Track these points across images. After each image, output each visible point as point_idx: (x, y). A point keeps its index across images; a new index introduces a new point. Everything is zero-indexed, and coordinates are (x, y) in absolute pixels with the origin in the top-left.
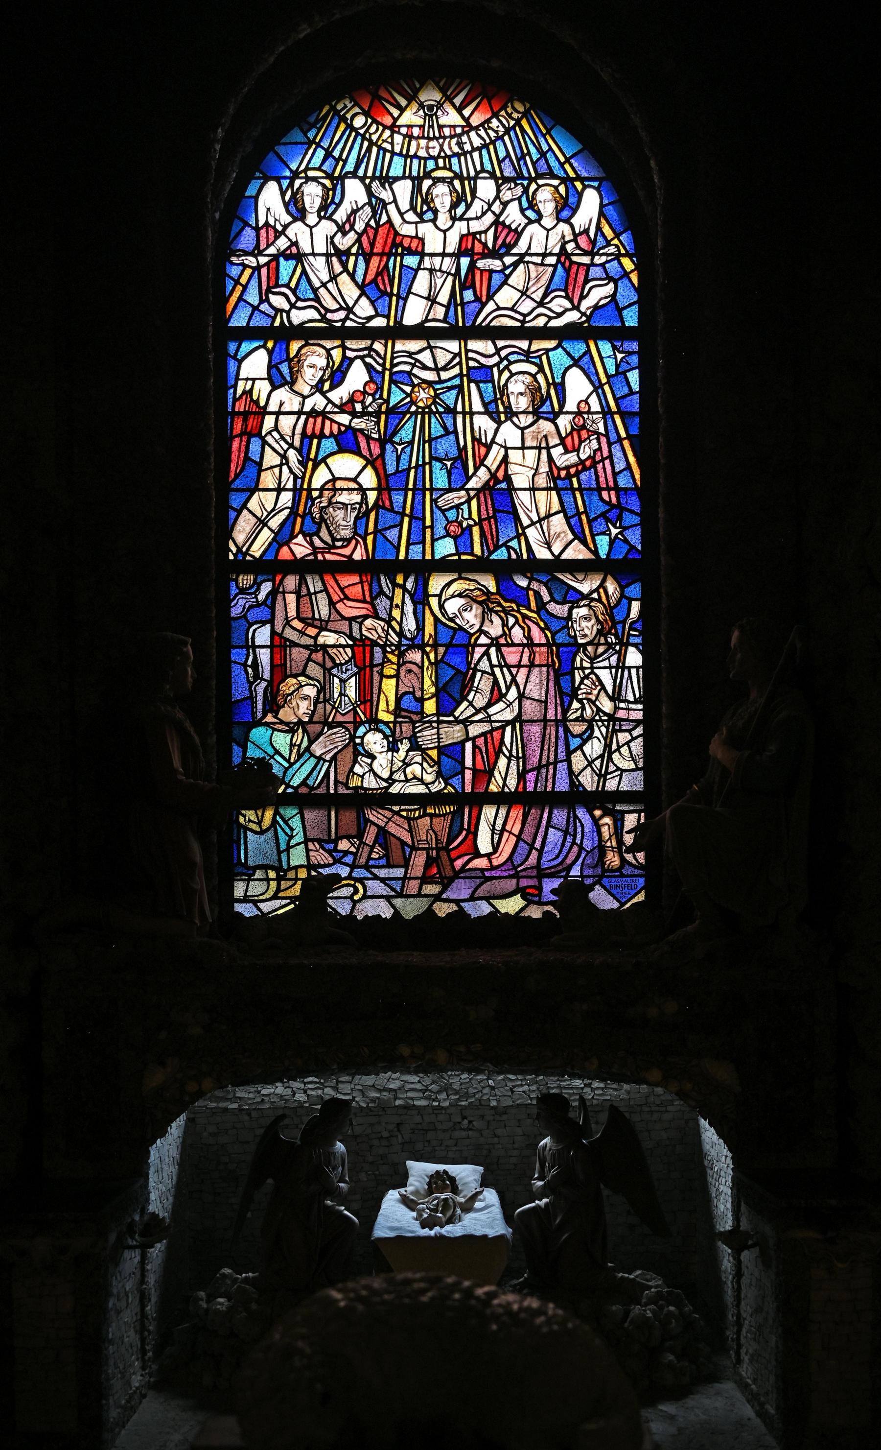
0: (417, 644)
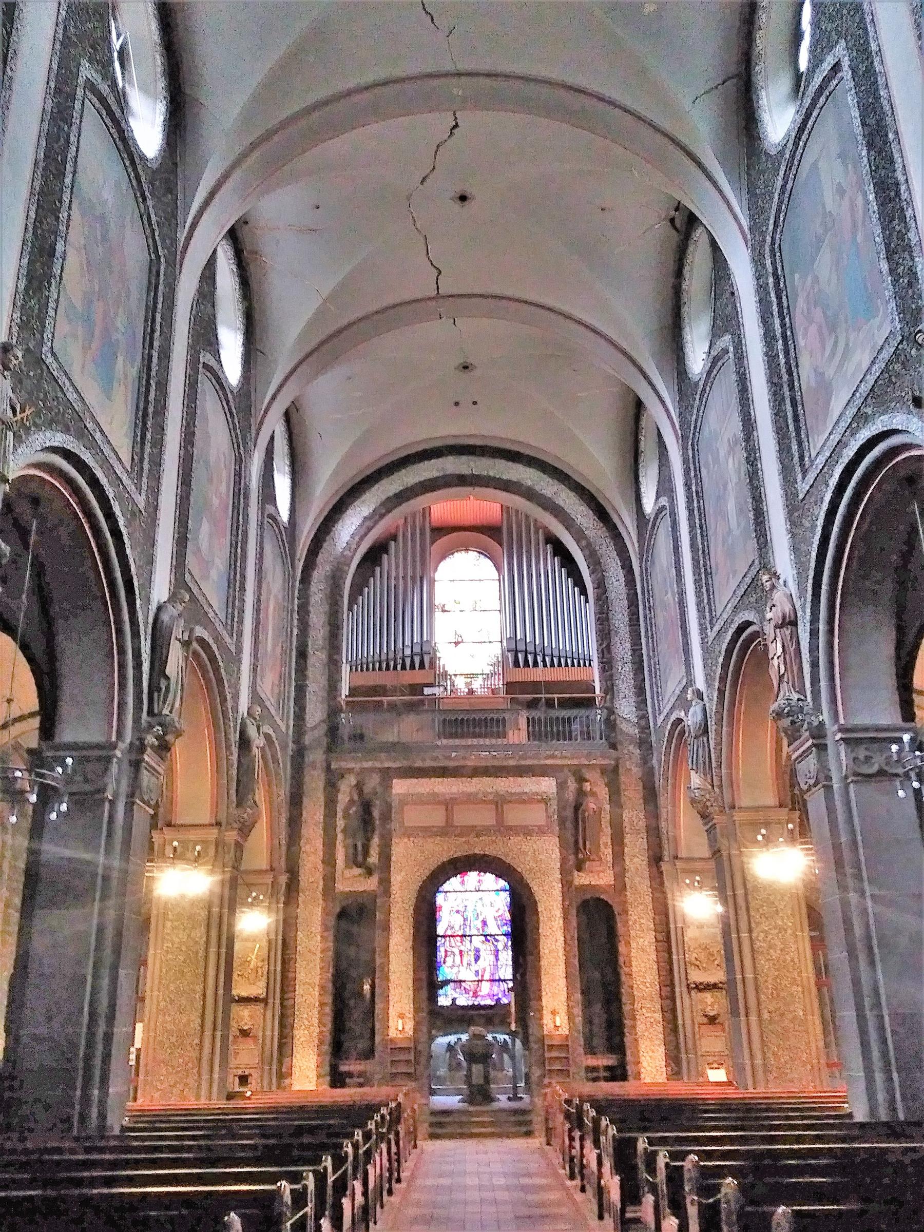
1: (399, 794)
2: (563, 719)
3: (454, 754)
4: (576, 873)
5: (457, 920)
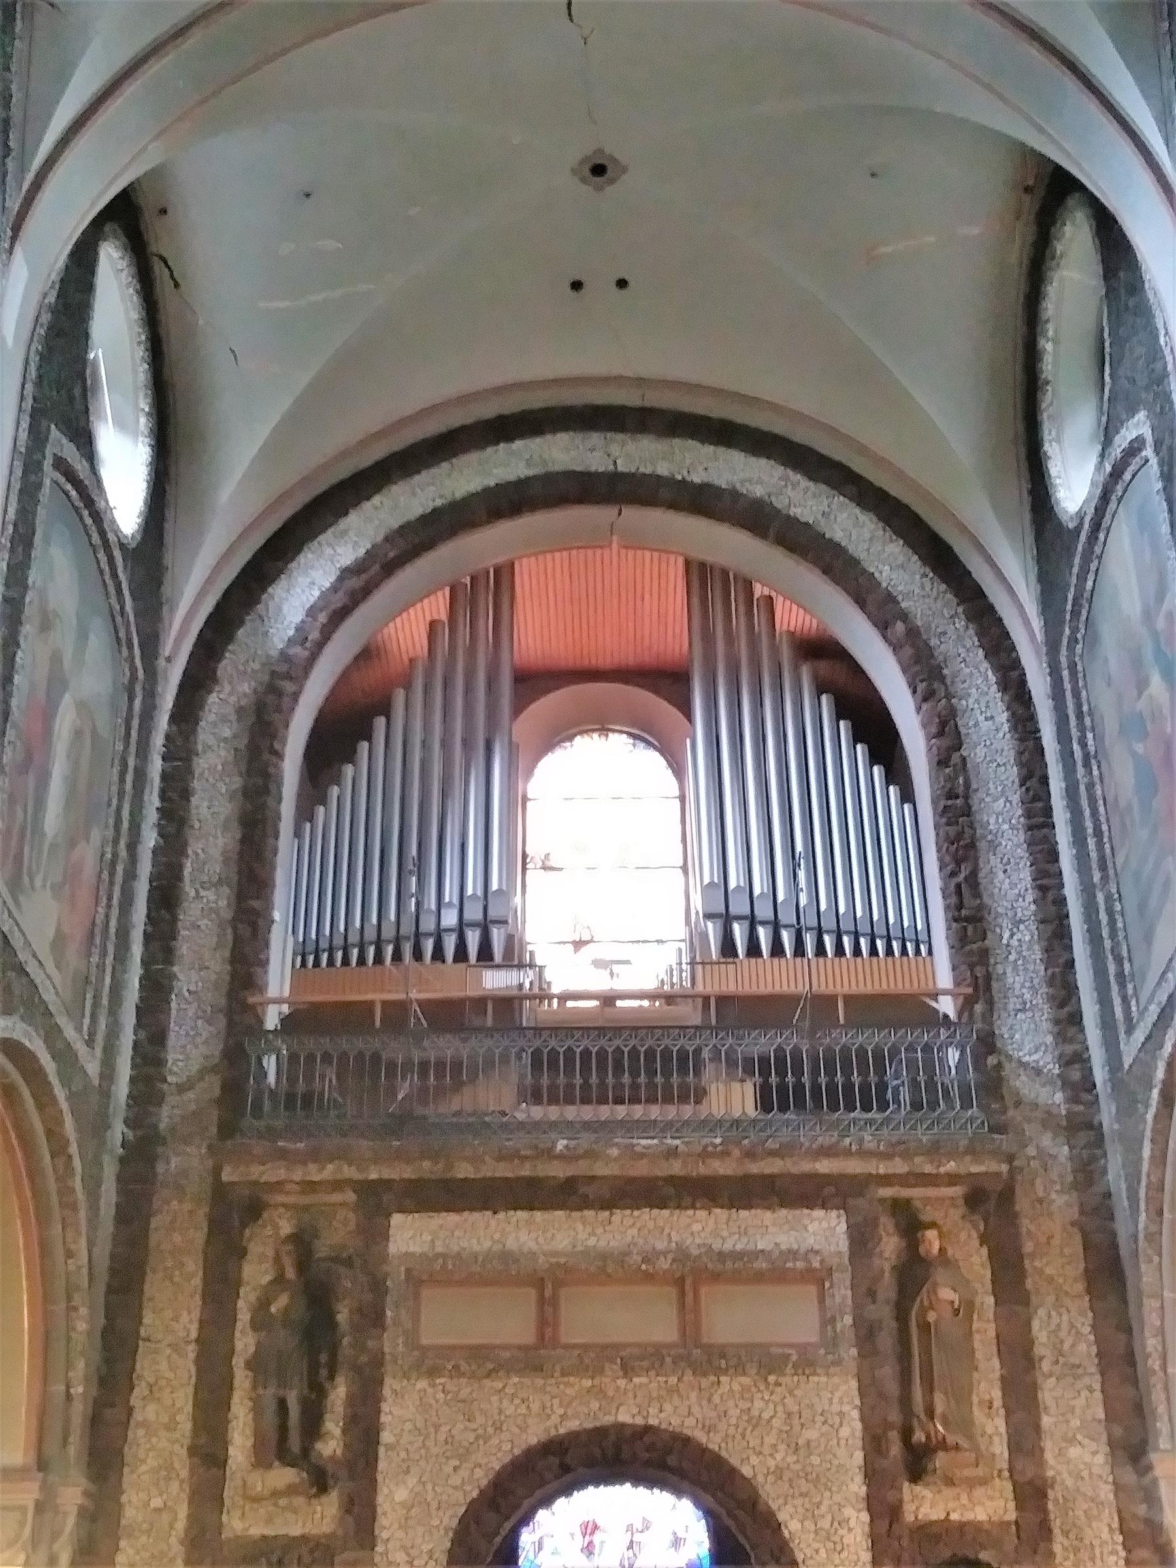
2: (862, 1053)
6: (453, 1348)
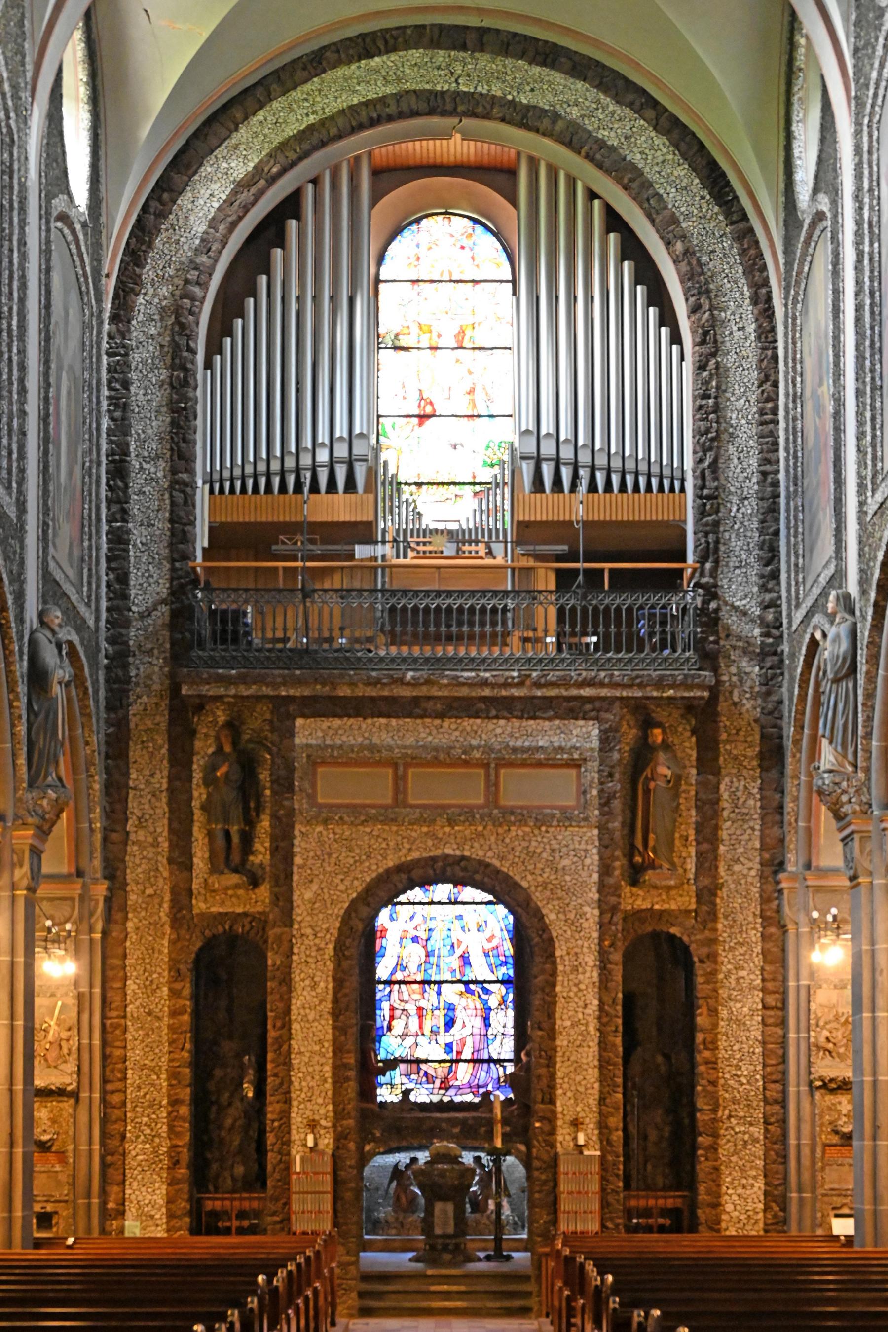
0: (438, 1008)
1: (308, 746)
3: (410, 674)
4: (628, 889)
5: (414, 954)
6: (339, 806)
